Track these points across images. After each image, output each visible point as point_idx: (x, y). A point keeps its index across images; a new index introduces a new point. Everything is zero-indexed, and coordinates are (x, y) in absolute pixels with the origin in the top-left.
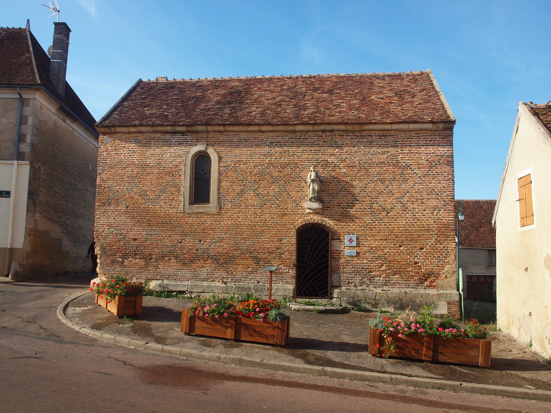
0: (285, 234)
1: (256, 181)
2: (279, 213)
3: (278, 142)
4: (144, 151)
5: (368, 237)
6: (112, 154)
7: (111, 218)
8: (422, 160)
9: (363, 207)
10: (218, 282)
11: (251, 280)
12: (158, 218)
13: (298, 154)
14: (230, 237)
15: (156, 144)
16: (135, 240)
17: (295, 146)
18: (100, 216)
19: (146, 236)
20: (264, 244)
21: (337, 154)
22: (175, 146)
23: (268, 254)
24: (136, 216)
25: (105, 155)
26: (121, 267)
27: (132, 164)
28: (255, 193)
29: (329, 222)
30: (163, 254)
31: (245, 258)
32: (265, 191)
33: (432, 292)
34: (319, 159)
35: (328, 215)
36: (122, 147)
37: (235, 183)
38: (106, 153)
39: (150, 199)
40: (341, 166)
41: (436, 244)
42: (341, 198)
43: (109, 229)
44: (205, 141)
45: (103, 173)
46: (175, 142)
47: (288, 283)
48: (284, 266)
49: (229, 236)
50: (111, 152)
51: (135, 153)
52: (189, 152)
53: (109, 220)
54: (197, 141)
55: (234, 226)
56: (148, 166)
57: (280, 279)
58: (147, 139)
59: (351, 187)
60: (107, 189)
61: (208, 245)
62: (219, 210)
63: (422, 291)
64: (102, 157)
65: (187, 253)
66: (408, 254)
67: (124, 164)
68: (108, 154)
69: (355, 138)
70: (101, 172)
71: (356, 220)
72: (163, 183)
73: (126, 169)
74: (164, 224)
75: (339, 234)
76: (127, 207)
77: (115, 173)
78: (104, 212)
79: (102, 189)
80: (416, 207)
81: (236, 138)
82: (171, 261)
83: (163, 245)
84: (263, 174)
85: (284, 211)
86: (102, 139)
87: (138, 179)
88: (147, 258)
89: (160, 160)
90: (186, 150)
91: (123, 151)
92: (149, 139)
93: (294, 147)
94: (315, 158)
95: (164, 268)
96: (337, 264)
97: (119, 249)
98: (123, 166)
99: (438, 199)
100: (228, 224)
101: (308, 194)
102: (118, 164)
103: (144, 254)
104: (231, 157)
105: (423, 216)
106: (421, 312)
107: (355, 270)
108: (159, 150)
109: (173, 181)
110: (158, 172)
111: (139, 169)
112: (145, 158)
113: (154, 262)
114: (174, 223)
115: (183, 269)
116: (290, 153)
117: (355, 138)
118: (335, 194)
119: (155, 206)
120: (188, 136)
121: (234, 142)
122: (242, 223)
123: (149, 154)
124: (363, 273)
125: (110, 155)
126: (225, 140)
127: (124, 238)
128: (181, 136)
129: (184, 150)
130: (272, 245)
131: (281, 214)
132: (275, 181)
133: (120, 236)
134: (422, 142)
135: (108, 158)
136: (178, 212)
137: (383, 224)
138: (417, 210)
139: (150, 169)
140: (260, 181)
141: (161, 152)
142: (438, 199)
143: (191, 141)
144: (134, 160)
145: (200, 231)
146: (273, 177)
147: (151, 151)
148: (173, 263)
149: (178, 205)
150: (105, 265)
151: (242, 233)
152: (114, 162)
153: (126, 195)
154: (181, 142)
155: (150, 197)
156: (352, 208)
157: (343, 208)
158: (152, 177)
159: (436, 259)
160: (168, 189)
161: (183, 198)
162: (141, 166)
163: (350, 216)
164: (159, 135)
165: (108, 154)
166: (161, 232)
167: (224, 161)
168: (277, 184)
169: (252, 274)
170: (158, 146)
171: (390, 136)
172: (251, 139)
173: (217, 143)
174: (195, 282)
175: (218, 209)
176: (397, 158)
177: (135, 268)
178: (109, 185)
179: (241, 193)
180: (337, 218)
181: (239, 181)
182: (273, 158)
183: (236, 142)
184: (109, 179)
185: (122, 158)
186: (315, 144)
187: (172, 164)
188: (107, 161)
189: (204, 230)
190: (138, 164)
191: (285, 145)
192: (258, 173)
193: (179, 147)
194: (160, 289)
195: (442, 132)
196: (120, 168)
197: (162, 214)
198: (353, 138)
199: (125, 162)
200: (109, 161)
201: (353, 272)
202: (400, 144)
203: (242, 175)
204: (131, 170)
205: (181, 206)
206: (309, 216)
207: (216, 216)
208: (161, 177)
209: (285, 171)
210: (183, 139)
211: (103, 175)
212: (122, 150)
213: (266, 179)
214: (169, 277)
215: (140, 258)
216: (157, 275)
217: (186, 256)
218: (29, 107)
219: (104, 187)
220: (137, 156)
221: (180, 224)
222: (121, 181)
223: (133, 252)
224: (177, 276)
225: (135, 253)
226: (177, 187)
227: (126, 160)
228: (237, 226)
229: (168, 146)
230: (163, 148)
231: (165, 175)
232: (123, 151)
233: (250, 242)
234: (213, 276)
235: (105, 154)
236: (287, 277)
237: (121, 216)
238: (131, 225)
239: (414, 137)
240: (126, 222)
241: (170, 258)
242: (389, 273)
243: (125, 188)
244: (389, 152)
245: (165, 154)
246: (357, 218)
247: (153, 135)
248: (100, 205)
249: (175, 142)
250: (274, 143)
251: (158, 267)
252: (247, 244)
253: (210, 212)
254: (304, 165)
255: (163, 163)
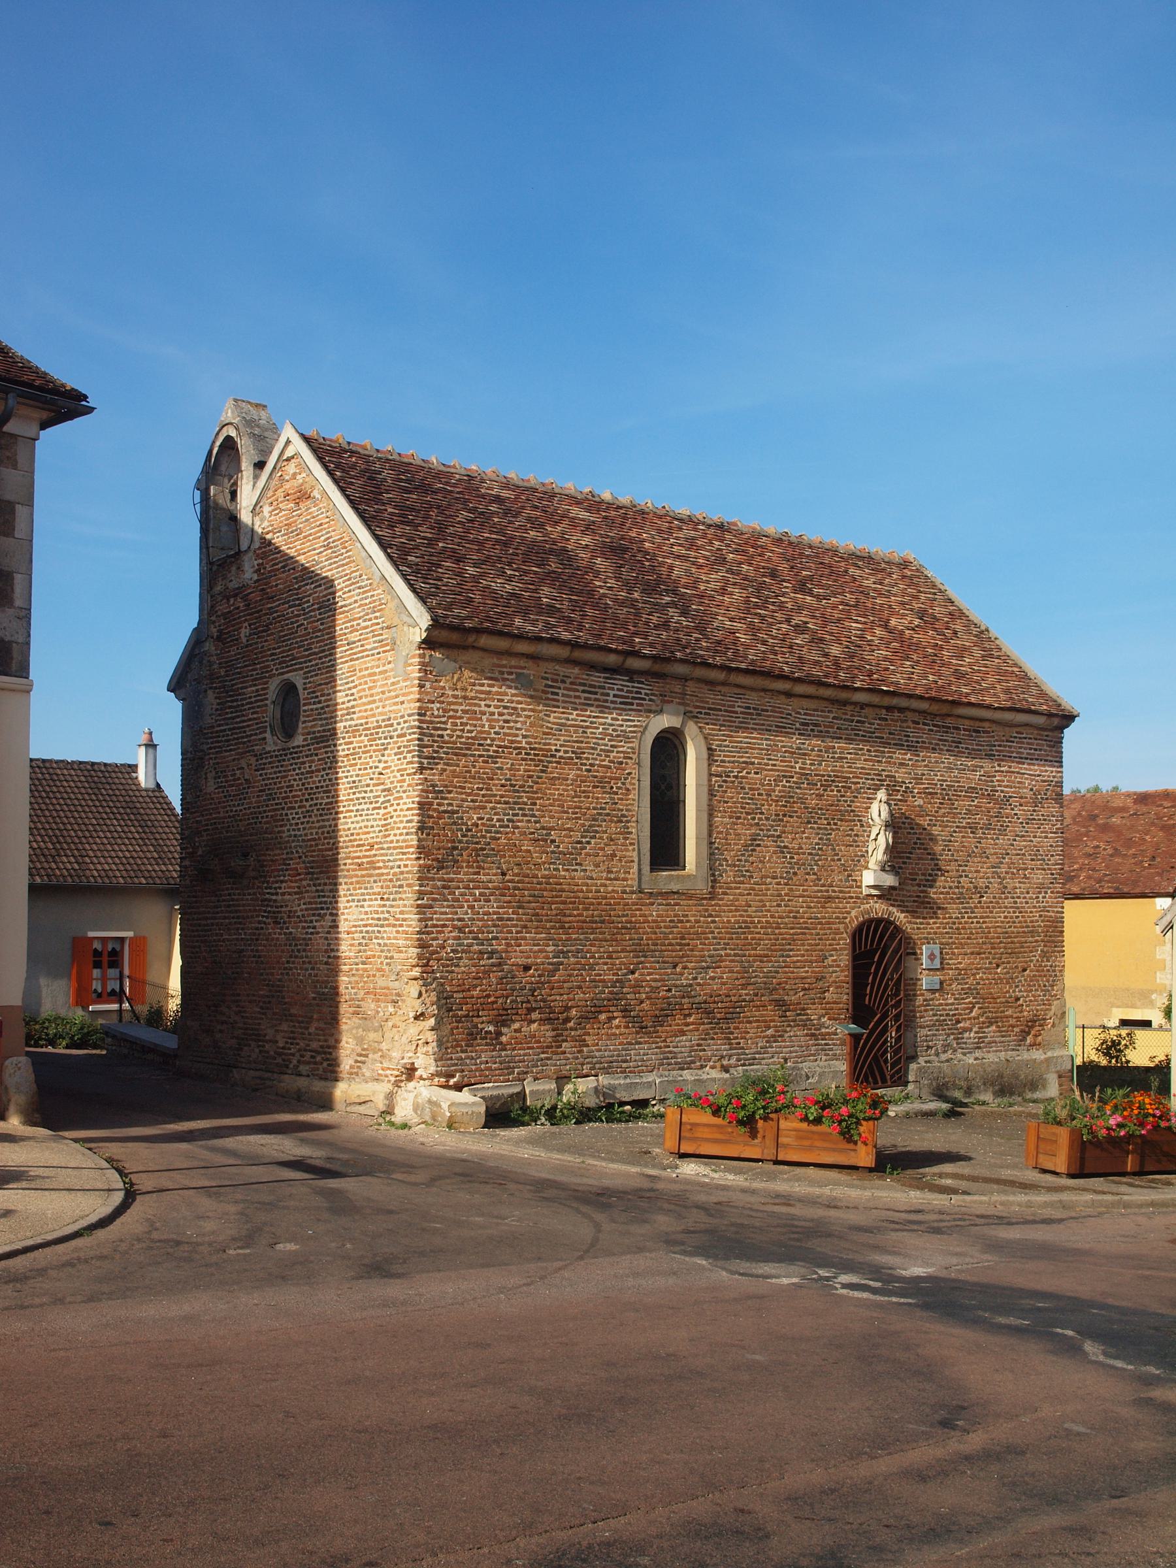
0: (830, 945)
1: (778, 815)
2: (819, 894)
3: (816, 725)
4: (541, 711)
5: (956, 948)
6: (457, 711)
7: (462, 907)
8: (1025, 788)
9: (947, 885)
10: (712, 1067)
11: (773, 1057)
12: (581, 906)
13: (849, 756)
14: (735, 955)
15: (570, 696)
16: (527, 968)
17: (844, 737)
18: (434, 900)
19: (554, 958)
20: (795, 970)
21: (910, 763)
22: (615, 708)
23: (801, 994)
24: (529, 902)
25: (436, 713)
26: (493, 1051)
27: (511, 747)
28: (779, 847)
29: (900, 917)
30: (595, 1006)
31: (762, 1003)
32: (795, 841)
33: (1038, 1055)
34: (883, 773)
35: (897, 901)
36: (482, 692)
37: (739, 818)
38: (438, 705)
39: (560, 853)
40: (916, 791)
41: (1042, 961)
42: (916, 864)
43: (459, 938)
44: (679, 704)
45: (432, 769)
46: (615, 696)
47: (835, 1057)
48: (829, 1019)
49: (732, 952)
50: (454, 704)
51: (519, 715)
52: (646, 728)
53: (456, 913)
54: (664, 702)
55: (740, 927)
56: (552, 756)
57: (822, 1050)
58: (547, 679)
59: (930, 839)
60: (447, 819)
61: (690, 977)
62: (713, 887)
63: (1026, 1056)
64: (427, 718)
65: (647, 998)
66: (1008, 983)
67: (491, 745)
68: (445, 711)
69: (937, 731)
70: (429, 763)
71: (939, 912)
72: (588, 809)
73: (496, 763)
74: (596, 922)
75: (914, 943)
76: (504, 874)
77: (466, 772)
78: (444, 887)
79: (432, 817)
80: (1017, 885)
81: (740, 704)
82: (614, 1022)
83: (594, 981)
84: (792, 800)
85: (827, 891)
86: (427, 660)
87: (528, 792)
88: (558, 1019)
89: (582, 742)
90: (639, 721)
91: (486, 705)
92: (553, 680)
93: (841, 738)
94: (875, 770)
95: (597, 1045)
96: (911, 1008)
97: (488, 996)
98: (488, 750)
99: (1044, 869)
100: (729, 922)
101: (867, 852)
102: (474, 744)
103: (550, 1007)
104: (732, 752)
105: (1027, 903)
106: (1028, 1097)
107: (937, 1021)
108: (577, 715)
109: (613, 804)
110: (578, 776)
111: (530, 765)
112: (545, 733)
113: (576, 1029)
114: (619, 919)
115: (640, 1043)
116: (836, 753)
117: (937, 731)
118: (906, 852)
119: (573, 874)
120: (642, 683)
121: (736, 712)
122: (756, 920)
123: (554, 723)
124: (947, 1025)
125: (451, 713)
126: (718, 704)
127: (500, 964)
128: (628, 681)
129: (634, 721)
130: (807, 972)
131: (822, 897)
132: (812, 817)
133: (489, 958)
134: (1025, 751)
135: (444, 723)
136: (628, 889)
137: (975, 920)
138: (1018, 890)
139: (556, 768)
140: (784, 815)
141: (582, 721)
142: (1044, 869)
143: (650, 700)
144: (517, 736)
145: (673, 941)
146: (807, 808)
147: (556, 715)
148: (618, 1027)
149: (625, 873)
150: (452, 1046)
151: (756, 944)
152: (462, 737)
153: (499, 839)
154: (627, 697)
155: (558, 847)
156: (931, 887)
157: (919, 885)
158: (563, 790)
159: (1042, 991)
160: (601, 826)
161: (635, 854)
162: (535, 755)
163: (929, 903)
164: (576, 671)
165: (445, 711)
166: (591, 945)
167: (717, 761)
168: (815, 826)
169: (775, 1042)
170: (576, 703)
171: (984, 732)
172: (767, 711)
173: (703, 711)
174: (667, 1073)
175: (710, 884)
176: (993, 781)
177: (529, 1048)
178: (451, 805)
179: (752, 845)
180: (911, 906)
181: (747, 813)
182: (808, 762)
183: (741, 713)
184: (451, 786)
185: (483, 726)
186: (876, 737)
187: (609, 756)
188: (445, 733)
189: (682, 938)
190: (526, 749)
191: (828, 732)
192: (781, 796)
193: (624, 713)
194: (597, 1101)
195: (1050, 733)
196: (480, 756)
197: (590, 895)
198: (932, 731)
199: (493, 740)
200: (448, 732)
201: (934, 1025)
202: (997, 751)
203: (752, 799)
204: (509, 766)
205: (633, 873)
206: (867, 903)
207: (705, 902)
208: (584, 792)
209: (828, 796)
210: (631, 692)
211: (434, 775)
212: (483, 703)
213: (796, 812)
214: (610, 1067)
215: (541, 1020)
216: (583, 1064)
217: (646, 1006)
218: (15, 467)
219: (439, 812)
220: (524, 727)
221: (631, 922)
222: (483, 796)
223: (522, 1003)
224: (626, 1061)
225: (529, 1005)
226: (622, 822)
227: (495, 733)
228: (747, 926)
229: (598, 706)
230: (586, 711)
231: (594, 787)
232: (486, 705)
233: (770, 964)
234: (701, 1054)
235: (438, 709)
236: (834, 1044)
237: (490, 901)
238: (515, 926)
239: (1016, 740)
240: (501, 919)
241: (611, 1015)
242: (983, 1023)
243: (495, 818)
244: (982, 767)
245: (591, 728)
246: (939, 908)
247: (563, 670)
248: (430, 866)
249: (615, 696)
250: (807, 724)
251: (584, 1040)
252: (765, 970)
253: (693, 892)
254: (859, 783)
255: (589, 753)
